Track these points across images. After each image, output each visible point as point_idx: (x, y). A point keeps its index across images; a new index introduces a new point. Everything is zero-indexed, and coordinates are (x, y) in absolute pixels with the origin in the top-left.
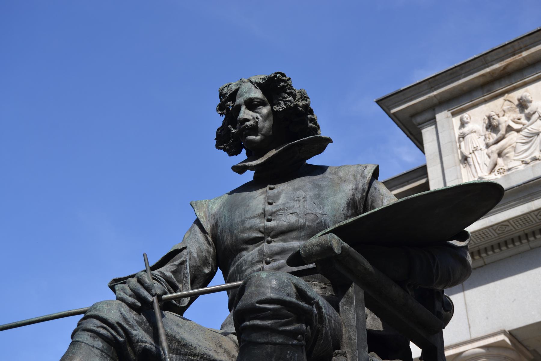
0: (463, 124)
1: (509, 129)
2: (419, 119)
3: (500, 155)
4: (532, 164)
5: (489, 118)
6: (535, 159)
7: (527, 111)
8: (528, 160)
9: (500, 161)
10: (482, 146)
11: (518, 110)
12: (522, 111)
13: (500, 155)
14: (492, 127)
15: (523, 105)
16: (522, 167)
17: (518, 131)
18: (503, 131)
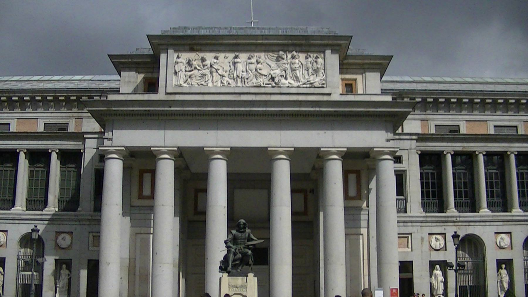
0: (178, 57)
1: (196, 68)
2: (161, 47)
3: (190, 77)
4: (201, 86)
5: (189, 60)
6: (202, 84)
7: (204, 63)
8: (199, 84)
9: (189, 80)
10: (184, 70)
11: (200, 61)
12: (202, 62)
13: (190, 77)
14: (189, 63)
15: (203, 60)
16: (197, 86)
17: (198, 70)
18: (193, 68)
